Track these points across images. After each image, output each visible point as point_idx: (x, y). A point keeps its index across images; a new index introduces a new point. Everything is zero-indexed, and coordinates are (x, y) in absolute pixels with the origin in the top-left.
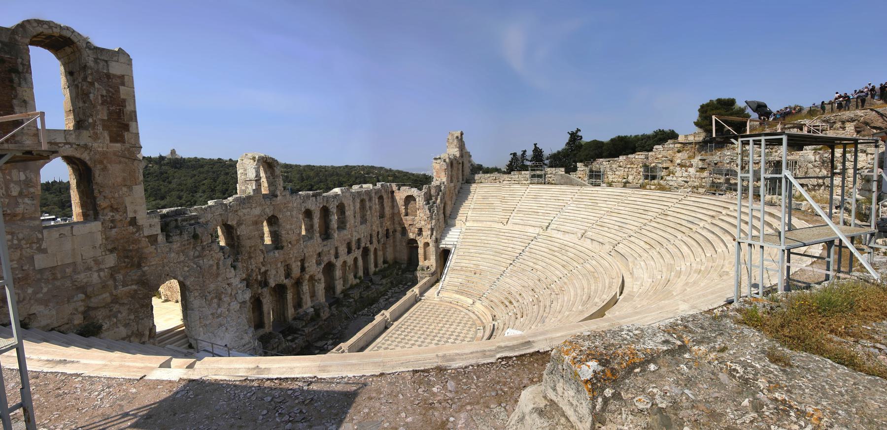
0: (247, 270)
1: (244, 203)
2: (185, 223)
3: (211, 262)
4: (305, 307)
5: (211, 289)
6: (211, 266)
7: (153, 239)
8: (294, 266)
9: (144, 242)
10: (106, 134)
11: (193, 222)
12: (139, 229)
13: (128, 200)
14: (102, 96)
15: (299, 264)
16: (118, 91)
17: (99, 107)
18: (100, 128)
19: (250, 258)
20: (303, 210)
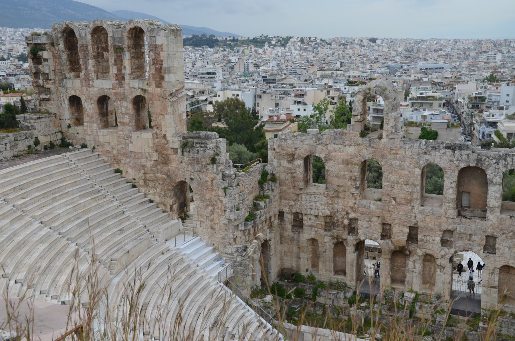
0: (333, 208)
1: (335, 139)
2: (198, 145)
3: (207, 179)
4: (407, 287)
5: (207, 198)
6: (207, 181)
7: (175, 150)
8: (395, 229)
9: (170, 152)
10: (154, 83)
11: (203, 145)
12: (168, 143)
13: (163, 123)
14: (153, 59)
15: (407, 230)
16: (159, 55)
17: (152, 67)
18: (151, 79)
19: (338, 197)
20: (422, 162)
